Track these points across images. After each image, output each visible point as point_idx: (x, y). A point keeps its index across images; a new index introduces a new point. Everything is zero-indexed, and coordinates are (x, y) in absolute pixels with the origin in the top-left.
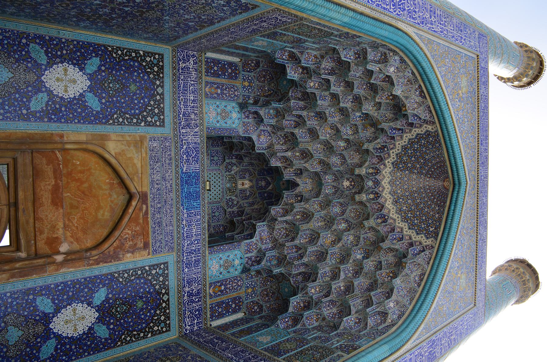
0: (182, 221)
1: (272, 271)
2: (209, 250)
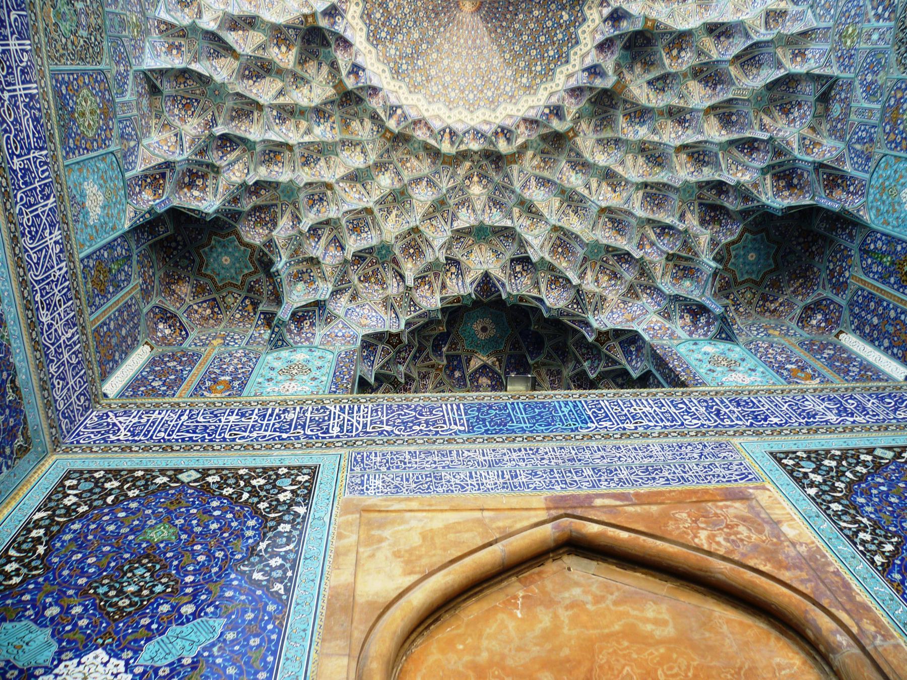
0: (624, 429)
1: (715, 274)
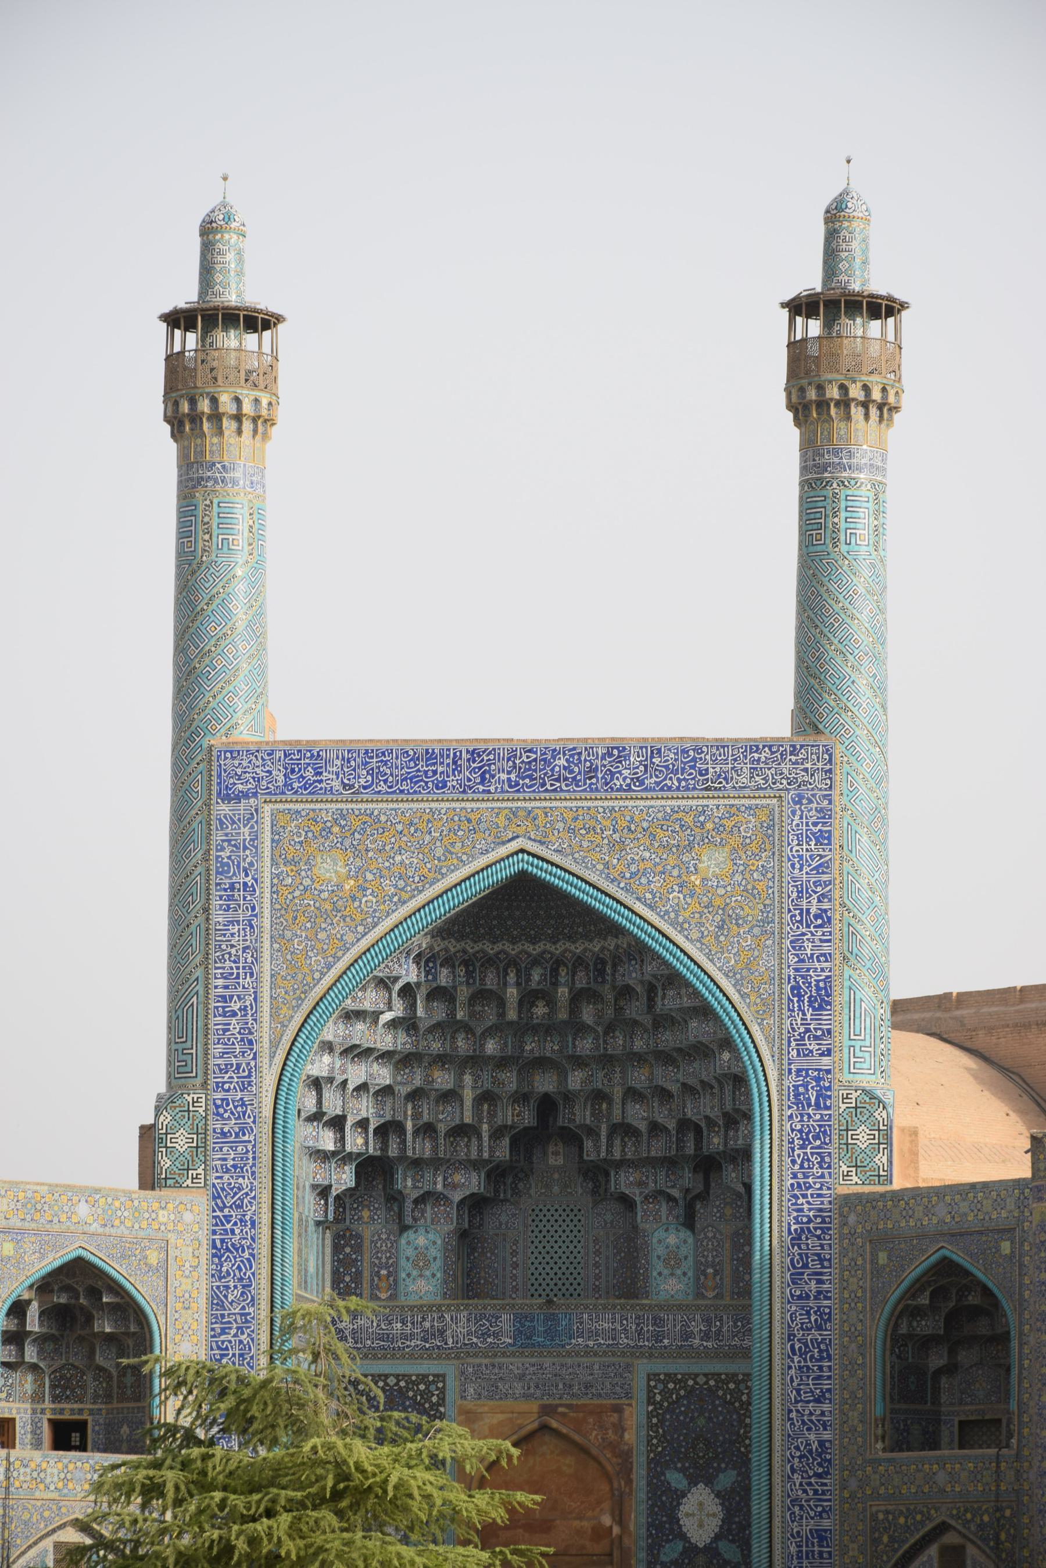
0: (587, 1346)
2: (642, 1298)
